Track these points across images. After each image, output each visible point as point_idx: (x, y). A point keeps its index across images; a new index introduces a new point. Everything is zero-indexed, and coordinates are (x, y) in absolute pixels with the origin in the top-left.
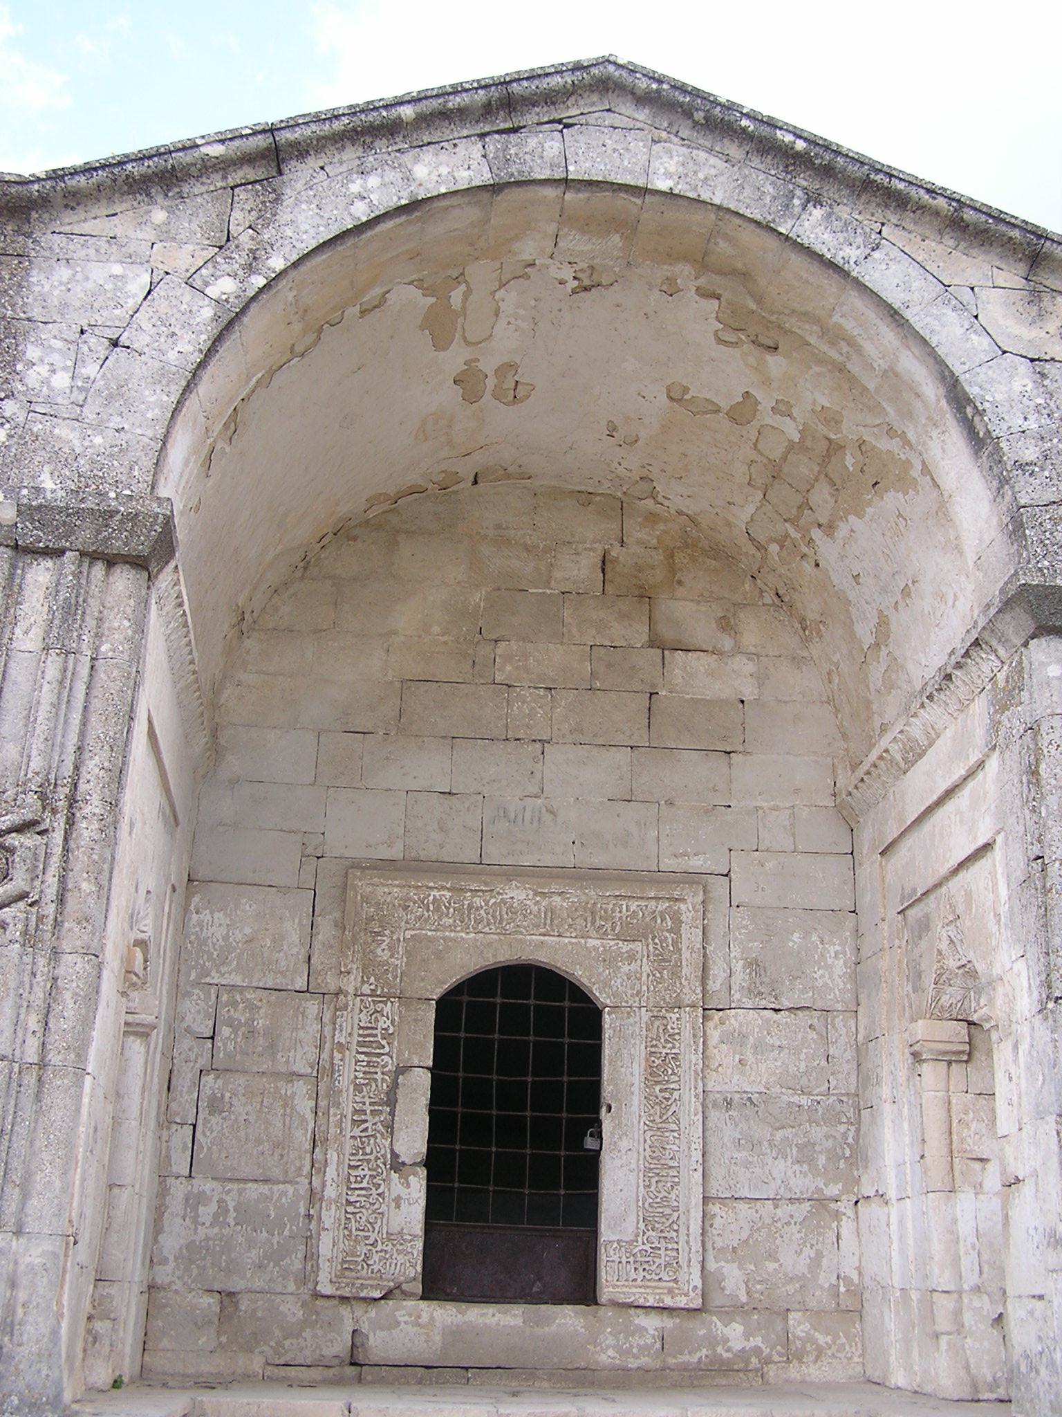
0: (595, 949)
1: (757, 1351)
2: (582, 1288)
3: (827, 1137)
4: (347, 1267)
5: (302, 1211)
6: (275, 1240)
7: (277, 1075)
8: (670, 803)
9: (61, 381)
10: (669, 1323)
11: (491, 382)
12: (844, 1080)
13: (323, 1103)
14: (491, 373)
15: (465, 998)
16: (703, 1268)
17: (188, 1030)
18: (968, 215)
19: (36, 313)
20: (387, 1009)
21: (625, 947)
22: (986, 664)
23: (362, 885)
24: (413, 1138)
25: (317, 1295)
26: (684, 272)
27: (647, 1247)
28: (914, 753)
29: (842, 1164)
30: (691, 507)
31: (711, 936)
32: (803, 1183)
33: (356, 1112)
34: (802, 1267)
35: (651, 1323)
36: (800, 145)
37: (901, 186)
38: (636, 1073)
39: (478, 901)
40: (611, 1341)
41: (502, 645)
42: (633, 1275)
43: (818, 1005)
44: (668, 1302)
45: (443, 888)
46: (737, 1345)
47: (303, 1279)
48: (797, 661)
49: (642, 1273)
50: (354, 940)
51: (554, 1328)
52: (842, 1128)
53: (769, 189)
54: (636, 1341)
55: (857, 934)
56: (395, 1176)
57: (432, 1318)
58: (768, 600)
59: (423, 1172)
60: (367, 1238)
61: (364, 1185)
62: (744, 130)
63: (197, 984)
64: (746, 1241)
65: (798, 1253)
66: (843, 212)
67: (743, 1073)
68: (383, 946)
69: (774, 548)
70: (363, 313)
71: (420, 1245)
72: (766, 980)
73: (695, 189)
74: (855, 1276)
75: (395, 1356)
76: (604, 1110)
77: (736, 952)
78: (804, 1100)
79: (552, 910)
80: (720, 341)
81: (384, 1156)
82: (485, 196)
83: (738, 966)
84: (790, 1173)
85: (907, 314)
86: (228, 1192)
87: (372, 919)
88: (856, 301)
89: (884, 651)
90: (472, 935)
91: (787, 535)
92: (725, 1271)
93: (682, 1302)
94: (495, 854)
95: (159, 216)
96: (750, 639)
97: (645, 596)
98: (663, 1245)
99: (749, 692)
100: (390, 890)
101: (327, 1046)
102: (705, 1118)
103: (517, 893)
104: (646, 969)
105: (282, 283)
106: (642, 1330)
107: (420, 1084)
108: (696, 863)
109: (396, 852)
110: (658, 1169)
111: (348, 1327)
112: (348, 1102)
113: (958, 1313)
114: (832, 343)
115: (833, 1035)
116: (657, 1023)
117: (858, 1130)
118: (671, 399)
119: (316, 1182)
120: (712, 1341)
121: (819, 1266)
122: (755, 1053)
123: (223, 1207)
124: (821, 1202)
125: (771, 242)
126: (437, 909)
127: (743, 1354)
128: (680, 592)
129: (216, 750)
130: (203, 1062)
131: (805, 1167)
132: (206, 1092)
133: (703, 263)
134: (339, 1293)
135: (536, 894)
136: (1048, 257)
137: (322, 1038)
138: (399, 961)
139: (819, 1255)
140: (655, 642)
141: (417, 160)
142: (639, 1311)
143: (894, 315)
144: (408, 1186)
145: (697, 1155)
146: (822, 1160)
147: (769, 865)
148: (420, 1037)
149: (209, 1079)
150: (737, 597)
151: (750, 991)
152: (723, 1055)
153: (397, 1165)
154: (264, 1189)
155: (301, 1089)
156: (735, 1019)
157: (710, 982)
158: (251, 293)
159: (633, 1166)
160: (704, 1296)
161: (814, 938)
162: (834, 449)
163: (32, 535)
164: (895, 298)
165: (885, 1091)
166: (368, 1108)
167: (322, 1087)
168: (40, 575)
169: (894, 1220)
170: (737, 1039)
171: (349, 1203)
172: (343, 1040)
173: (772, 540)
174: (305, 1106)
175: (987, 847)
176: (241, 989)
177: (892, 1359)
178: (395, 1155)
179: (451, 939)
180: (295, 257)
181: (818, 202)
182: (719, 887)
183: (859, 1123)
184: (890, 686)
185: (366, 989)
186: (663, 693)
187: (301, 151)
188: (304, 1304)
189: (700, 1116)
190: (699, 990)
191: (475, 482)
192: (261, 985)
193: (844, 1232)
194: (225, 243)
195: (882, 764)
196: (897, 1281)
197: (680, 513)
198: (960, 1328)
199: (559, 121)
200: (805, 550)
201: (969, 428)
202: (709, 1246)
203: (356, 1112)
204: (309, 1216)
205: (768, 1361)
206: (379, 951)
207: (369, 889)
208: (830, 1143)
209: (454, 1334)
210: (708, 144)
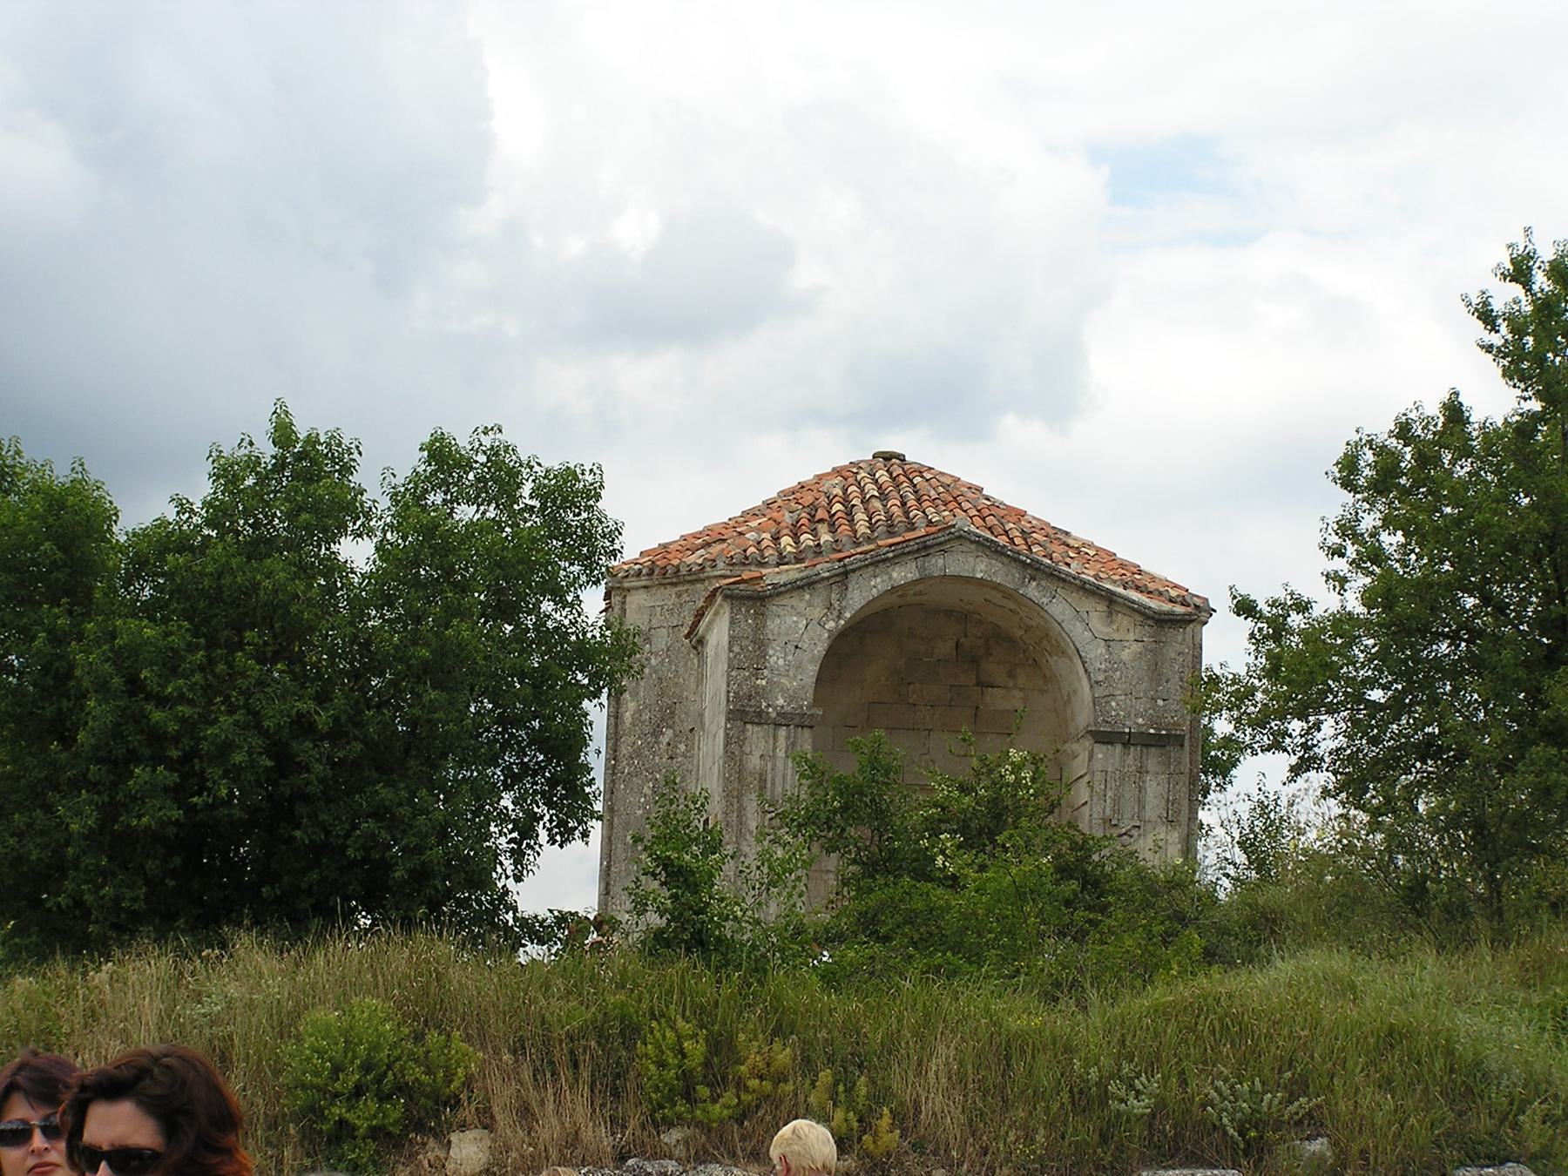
9: (781, 662)
48: (1042, 692)
66: (1043, 583)
95: (807, 597)
96: (1021, 681)
99: (1020, 706)
140: (979, 684)
155: (832, 876)
168: (782, 732)
187: (854, 571)
194: (830, 607)
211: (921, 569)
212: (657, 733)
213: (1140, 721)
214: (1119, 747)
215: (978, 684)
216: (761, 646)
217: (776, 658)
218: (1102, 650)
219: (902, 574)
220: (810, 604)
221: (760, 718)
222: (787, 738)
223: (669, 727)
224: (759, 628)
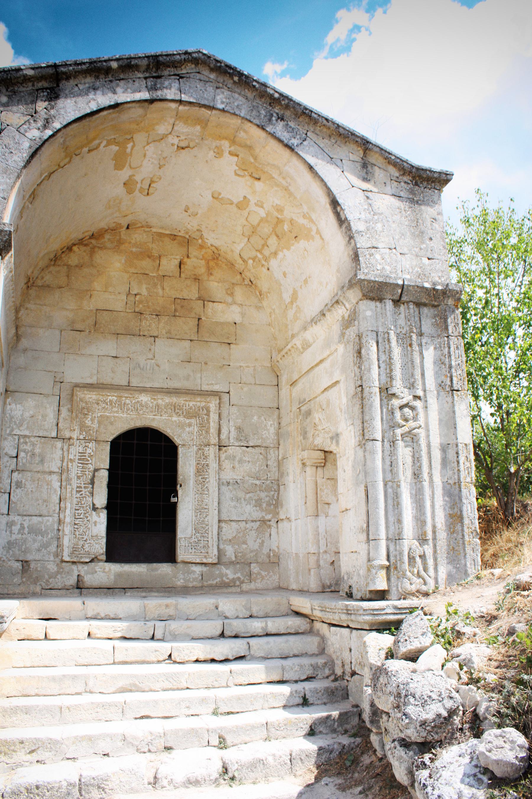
0: (175, 421)
1: (239, 578)
2: (170, 556)
3: (266, 496)
4: (74, 550)
5: (56, 527)
6: (45, 539)
7: (44, 472)
8: (206, 363)
10: (205, 569)
11: (139, 186)
13: (64, 484)
14: (139, 181)
15: (122, 441)
16: (218, 548)
17: (6, 454)
18: (341, 130)
20: (90, 445)
21: (188, 421)
23: (80, 394)
24: (101, 498)
25: (63, 561)
26: (226, 144)
27: (196, 540)
28: (306, 346)
29: (272, 507)
30: (217, 243)
31: (222, 417)
32: (257, 514)
33: (78, 487)
34: (256, 547)
35: (198, 569)
36: (276, 95)
37: (316, 116)
38: (192, 471)
39: (128, 401)
40: (182, 576)
41: (138, 297)
42: (190, 551)
43: (264, 445)
44: (205, 561)
45: (114, 396)
46: (231, 576)
47: (57, 555)
49: (194, 550)
50: (77, 416)
51: (159, 572)
52: (272, 493)
53: (263, 112)
54: (192, 576)
55: (279, 417)
56: (94, 513)
57: (110, 569)
58: (246, 283)
59: (105, 512)
60: (83, 538)
61: (82, 516)
62: (254, 86)
63: (10, 434)
64: (235, 537)
65: (255, 541)
66: (292, 124)
67: (234, 471)
68: (89, 419)
69: (250, 262)
70: (89, 151)
71: (105, 540)
72: (244, 435)
73: (233, 109)
74: (277, 550)
75: (96, 584)
76: (179, 486)
77: (231, 423)
78: (258, 482)
79: (158, 405)
80: (236, 174)
81: (90, 505)
82: (146, 104)
83: (233, 429)
84: (252, 510)
85: (316, 168)
86: (24, 520)
87: (84, 408)
89: (294, 306)
90: (125, 415)
91: (256, 256)
92: (227, 549)
93: (210, 561)
94: (135, 382)
97: (197, 279)
98: (202, 539)
99: (238, 319)
100: (91, 396)
101: (66, 460)
102: (219, 489)
103: (144, 398)
104: (196, 430)
105: (59, 134)
106: (194, 572)
107: (104, 475)
108: (216, 388)
109: (93, 380)
110: (201, 510)
111: (76, 573)
112: (75, 483)
113: (318, 561)
114: (284, 178)
115: (269, 457)
116: (200, 452)
117: (278, 494)
118: (213, 197)
119: (62, 516)
120: (221, 575)
121: (263, 546)
122: (239, 463)
123: (22, 527)
124: (264, 522)
126: (111, 404)
127: (234, 581)
128: (212, 278)
129: (18, 337)
130: (13, 467)
131: (258, 508)
132: (14, 479)
133: (233, 141)
134: (72, 560)
135: (152, 399)
137: (63, 457)
138: (95, 426)
139: (263, 542)
141: (118, 85)
142: (193, 565)
144: (99, 517)
145: (216, 504)
146: (264, 505)
147: (245, 389)
148: (104, 457)
149: (15, 475)
150: (234, 281)
151: (237, 439)
152: (227, 465)
153: (95, 509)
154: (40, 519)
156: (231, 450)
157: (221, 435)
158: (46, 137)
159: (190, 508)
160: (219, 558)
161: (263, 418)
162: (279, 221)
165: (291, 478)
166: (83, 486)
167: (64, 477)
169: (293, 528)
170: (232, 458)
171: (75, 524)
172: (72, 458)
173: (250, 258)
174: (57, 485)
175: (337, 382)
176: (29, 437)
177: (292, 580)
178: (94, 505)
179: (117, 417)
180: (65, 123)
181: (282, 119)
182: (225, 397)
183: (279, 491)
184: (296, 318)
185: (81, 437)
186: (203, 318)
188: (57, 565)
189: (217, 488)
190: (217, 439)
191: (128, 228)
192: (37, 435)
193: (272, 533)
195: (293, 350)
196: (294, 552)
197: (212, 245)
198: (319, 566)
199: (178, 75)
200: (264, 262)
201: (337, 215)
202: (220, 539)
203: (78, 487)
204: (59, 530)
205: (242, 582)
206: (87, 422)
207: (83, 396)
208: (267, 499)
209: (119, 575)
210: (239, 91)
214: (389, 304)
215: (199, 298)
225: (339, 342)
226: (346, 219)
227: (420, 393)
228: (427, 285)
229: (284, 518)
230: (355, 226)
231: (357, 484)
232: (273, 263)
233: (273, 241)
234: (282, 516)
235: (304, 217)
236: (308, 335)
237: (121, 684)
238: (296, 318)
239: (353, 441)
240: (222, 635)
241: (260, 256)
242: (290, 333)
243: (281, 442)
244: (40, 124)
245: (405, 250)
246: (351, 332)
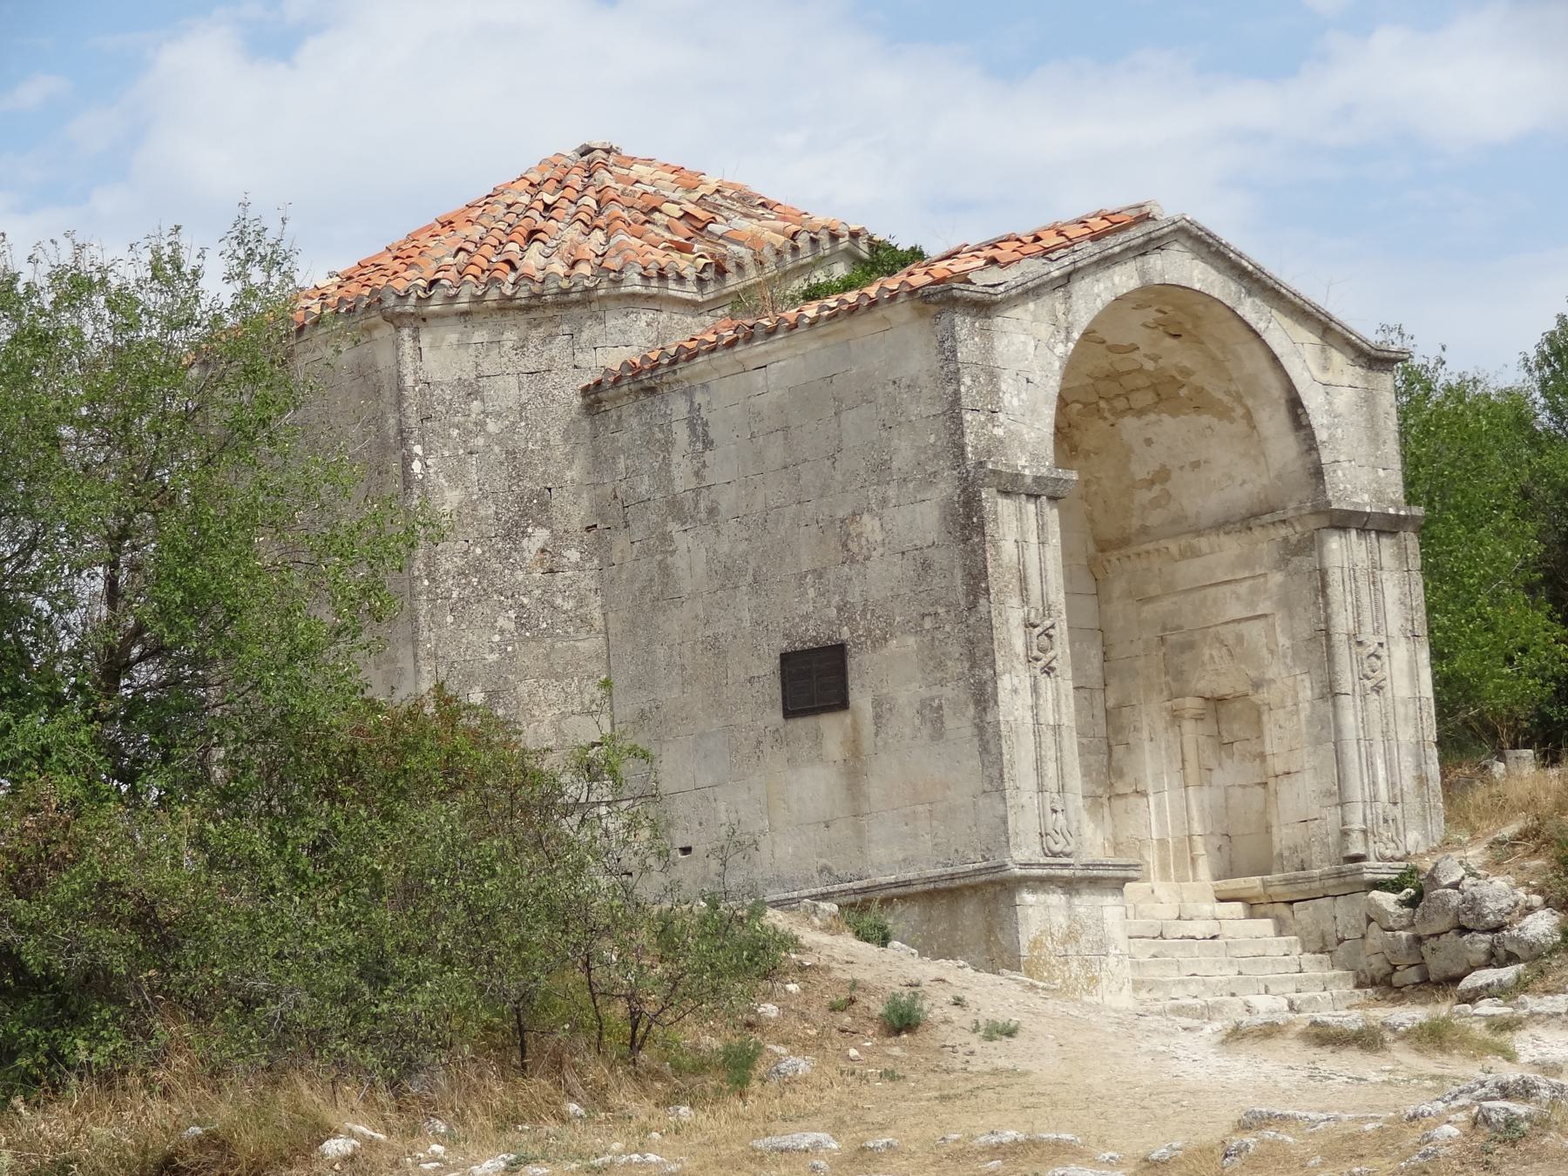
9: (1015, 402)
12: (1101, 729)
19: (1000, 363)
22: (1283, 531)
28: (1195, 553)
36: (1250, 268)
66: (1258, 301)
88: (1255, 345)
89: (1157, 488)
95: (1031, 306)
125: (1229, 314)
136: (1332, 330)
143: (1275, 359)
163: (1035, 489)
164: (1277, 351)
165: (1145, 735)
173: (1077, 401)
175: (1265, 616)
200: (1107, 414)
211: (1143, 273)
212: (514, 533)
213: (1366, 497)
214: (1354, 533)
216: (993, 376)
217: (1012, 396)
218: (1321, 398)
219: (1124, 279)
220: (1035, 319)
221: (1010, 487)
222: (1040, 514)
223: (540, 524)
224: (988, 350)
225: (1279, 569)
226: (1310, 426)
227: (1383, 640)
228: (1392, 511)
229: (1129, 790)
230: (1321, 435)
231: (1318, 741)
232: (1130, 423)
233: (1143, 399)
234: (1121, 788)
235: (1228, 393)
236: (1203, 543)
237: (1152, 951)
238: (1155, 503)
239: (1309, 693)
240: (1179, 918)
241: (1103, 404)
242: (1135, 523)
243: (1113, 682)
244: (1063, 336)
245: (1363, 461)
246: (1305, 563)
